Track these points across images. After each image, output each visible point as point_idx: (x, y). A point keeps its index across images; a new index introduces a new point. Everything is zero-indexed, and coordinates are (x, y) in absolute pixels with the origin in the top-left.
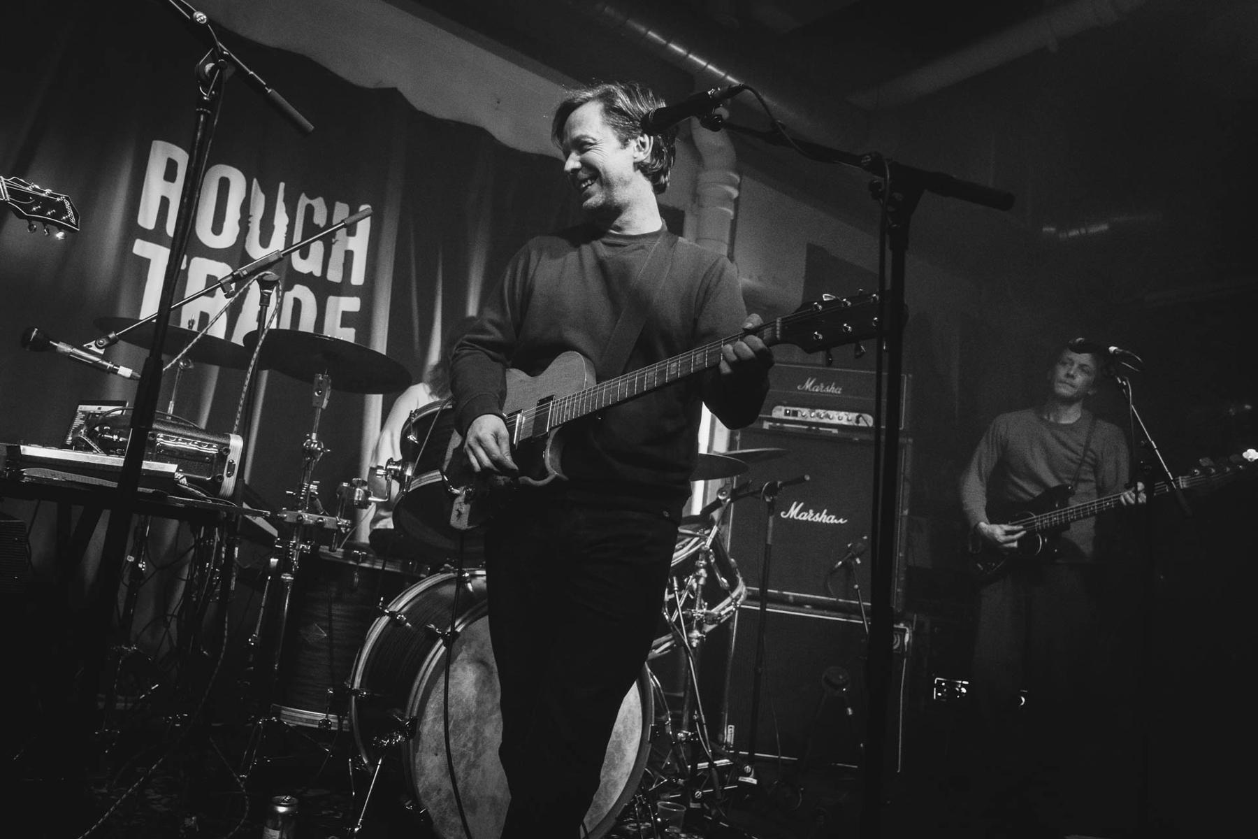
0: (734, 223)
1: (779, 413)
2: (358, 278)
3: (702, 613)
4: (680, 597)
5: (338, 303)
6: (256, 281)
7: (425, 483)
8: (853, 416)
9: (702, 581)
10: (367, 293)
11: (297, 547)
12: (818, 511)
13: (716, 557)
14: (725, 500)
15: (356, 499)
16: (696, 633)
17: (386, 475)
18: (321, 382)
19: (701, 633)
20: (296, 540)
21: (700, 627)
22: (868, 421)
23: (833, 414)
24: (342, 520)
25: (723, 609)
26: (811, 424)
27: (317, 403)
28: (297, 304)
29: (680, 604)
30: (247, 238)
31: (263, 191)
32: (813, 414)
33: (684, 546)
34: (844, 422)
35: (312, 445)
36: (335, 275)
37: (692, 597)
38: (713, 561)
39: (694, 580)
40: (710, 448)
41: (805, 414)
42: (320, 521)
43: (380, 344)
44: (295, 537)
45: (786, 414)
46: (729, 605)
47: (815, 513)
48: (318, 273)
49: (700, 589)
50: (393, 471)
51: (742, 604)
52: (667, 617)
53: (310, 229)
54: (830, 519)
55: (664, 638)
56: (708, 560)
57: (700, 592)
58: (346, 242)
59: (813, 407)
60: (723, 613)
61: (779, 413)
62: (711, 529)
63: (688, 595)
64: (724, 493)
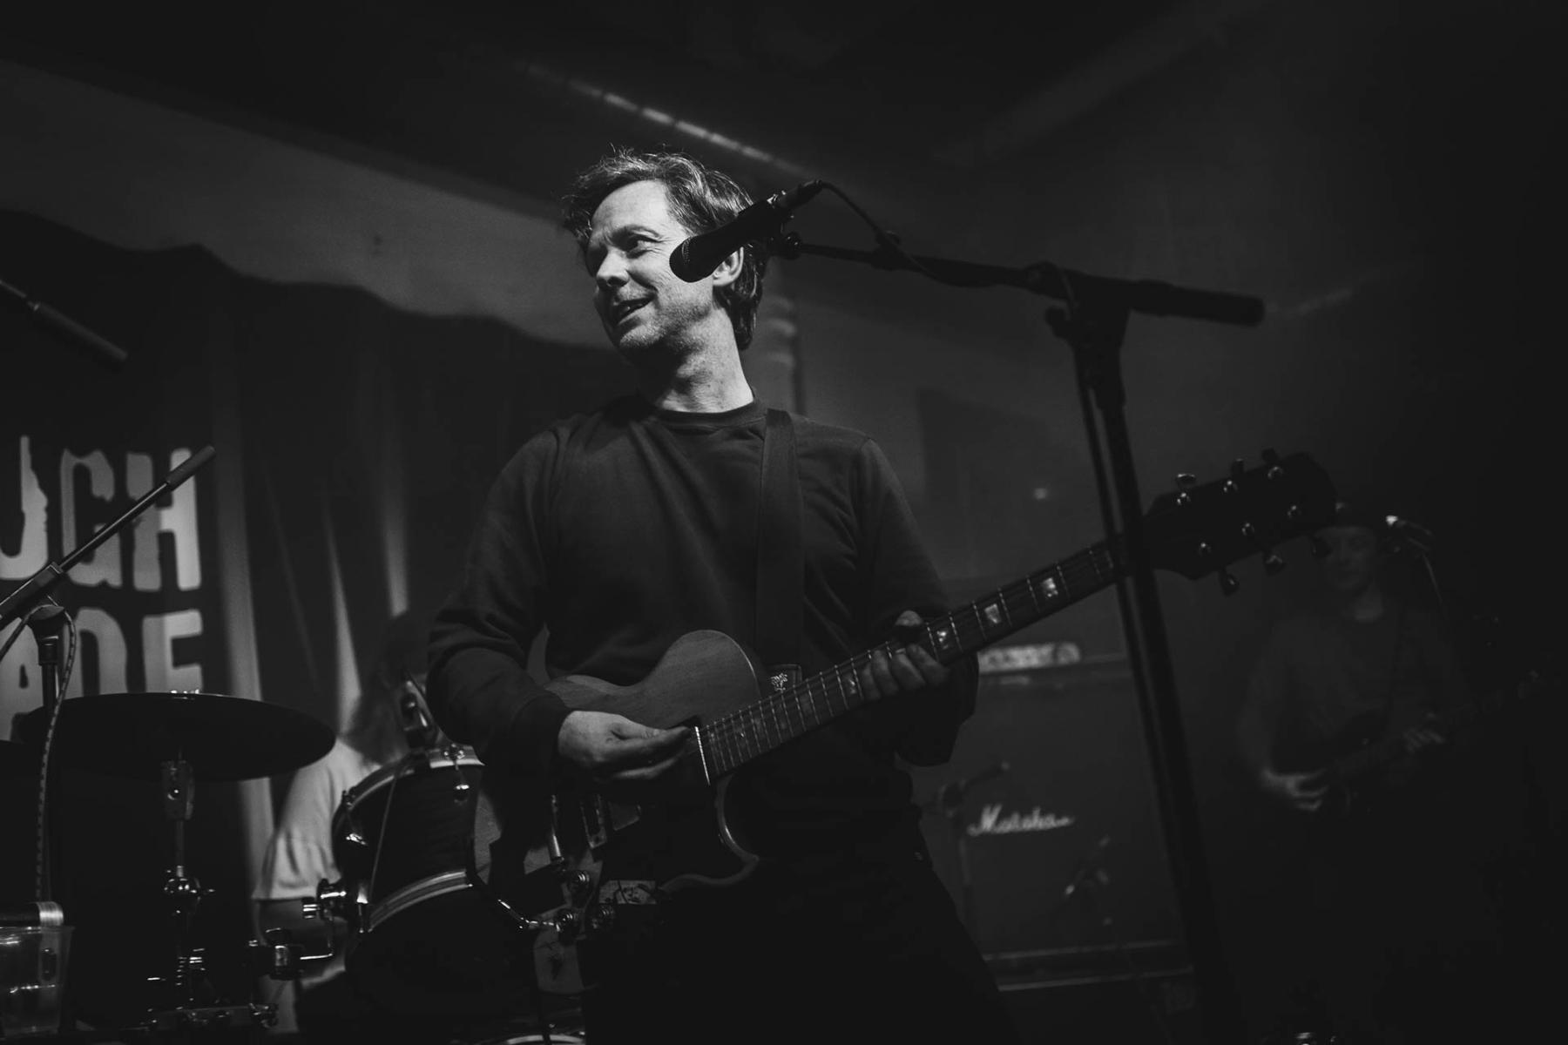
2: (189, 575)
5: (161, 629)
6: (27, 628)
7: (394, 911)
10: (208, 599)
12: (1026, 813)
15: (278, 964)
17: (321, 912)
24: (259, 1006)
28: (90, 642)
36: (147, 579)
42: (221, 1016)
43: (248, 685)
48: (115, 580)
50: (331, 903)
58: (157, 521)
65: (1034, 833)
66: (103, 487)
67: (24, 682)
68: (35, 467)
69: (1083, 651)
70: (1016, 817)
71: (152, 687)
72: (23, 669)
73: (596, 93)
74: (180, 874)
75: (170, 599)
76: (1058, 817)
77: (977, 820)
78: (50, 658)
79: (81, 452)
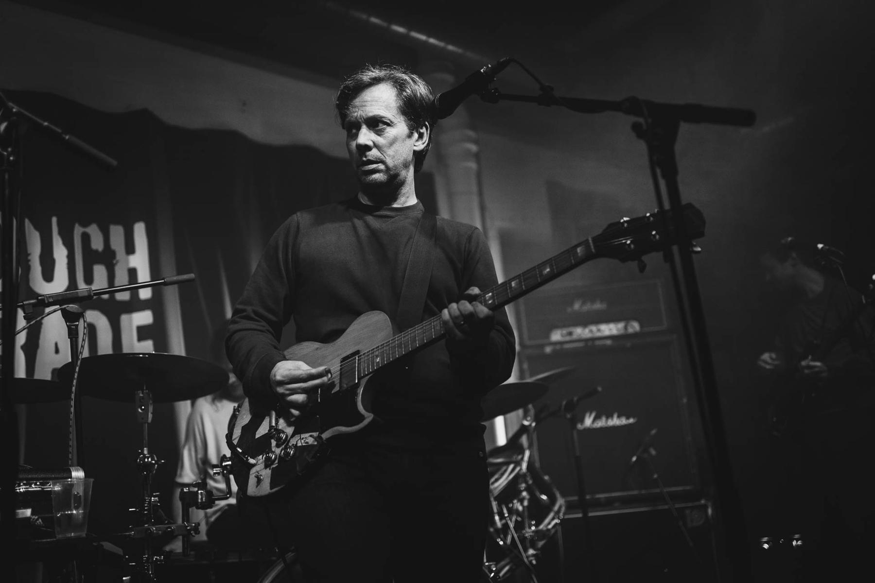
0: (479, 175)
1: (556, 336)
3: (533, 532)
4: (511, 520)
8: (621, 325)
9: (526, 503)
10: (156, 305)
11: (150, 561)
12: (609, 416)
13: (533, 478)
14: (530, 425)
16: (531, 552)
17: (223, 472)
18: (143, 398)
19: (535, 550)
20: (148, 555)
21: (533, 546)
22: (635, 327)
25: (550, 522)
26: (586, 340)
27: (143, 419)
28: (92, 329)
29: (512, 525)
30: (31, 276)
31: (36, 228)
32: (587, 330)
33: (502, 474)
35: (146, 460)
37: (519, 519)
38: (530, 482)
39: (519, 504)
41: (580, 332)
42: (169, 530)
44: (146, 551)
45: (562, 336)
46: (553, 519)
47: (607, 418)
49: (526, 509)
51: (565, 514)
52: (501, 543)
53: (91, 258)
54: (622, 421)
55: (503, 563)
56: (526, 482)
57: (526, 514)
58: (127, 262)
59: (585, 324)
60: (550, 527)
61: (556, 336)
62: (522, 452)
63: (516, 519)
65: (614, 428)
66: (97, 244)
67: (57, 351)
68: (60, 233)
69: (641, 326)
70: (604, 419)
71: (126, 350)
72: (56, 344)
74: (146, 452)
75: (135, 305)
76: (628, 418)
77: (582, 421)
78: (73, 334)
79: (85, 225)
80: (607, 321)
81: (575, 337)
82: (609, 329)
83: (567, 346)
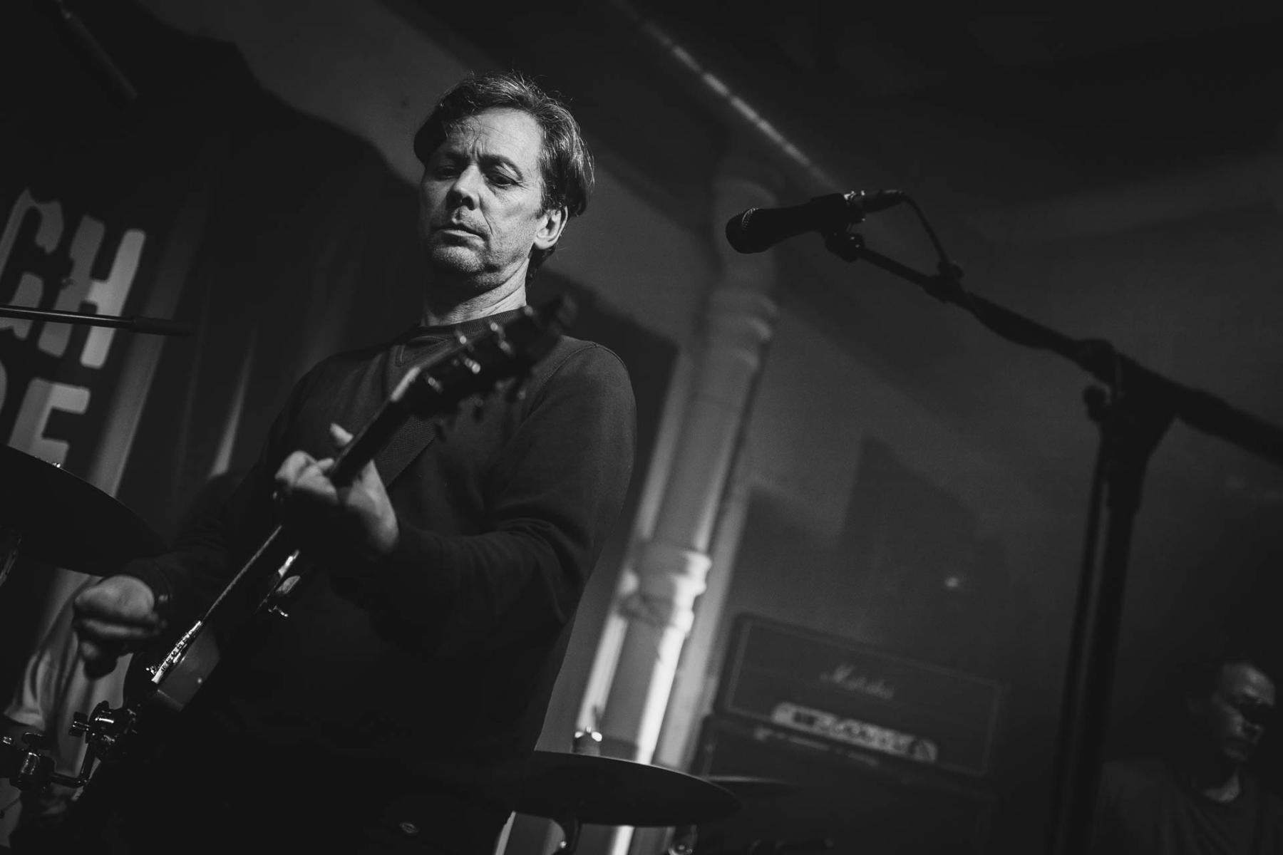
0: (755, 381)
1: (784, 715)
5: (45, 396)
8: (905, 740)
22: (928, 752)
23: (872, 731)
32: (842, 727)
34: (889, 748)
36: (53, 342)
40: (655, 756)
41: (828, 723)
45: (798, 718)
58: (87, 290)
59: (842, 715)
61: (784, 715)
64: (681, 848)
66: (48, 239)
73: (666, 41)
79: (42, 197)
80: (883, 724)
81: (816, 730)
82: (879, 738)
83: (796, 740)
